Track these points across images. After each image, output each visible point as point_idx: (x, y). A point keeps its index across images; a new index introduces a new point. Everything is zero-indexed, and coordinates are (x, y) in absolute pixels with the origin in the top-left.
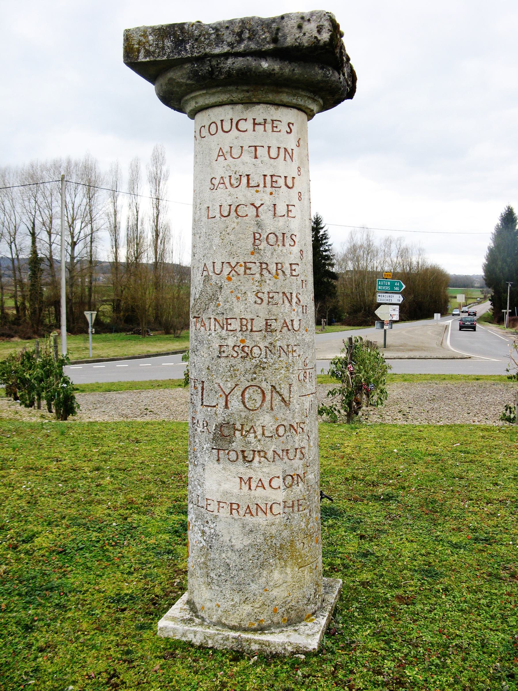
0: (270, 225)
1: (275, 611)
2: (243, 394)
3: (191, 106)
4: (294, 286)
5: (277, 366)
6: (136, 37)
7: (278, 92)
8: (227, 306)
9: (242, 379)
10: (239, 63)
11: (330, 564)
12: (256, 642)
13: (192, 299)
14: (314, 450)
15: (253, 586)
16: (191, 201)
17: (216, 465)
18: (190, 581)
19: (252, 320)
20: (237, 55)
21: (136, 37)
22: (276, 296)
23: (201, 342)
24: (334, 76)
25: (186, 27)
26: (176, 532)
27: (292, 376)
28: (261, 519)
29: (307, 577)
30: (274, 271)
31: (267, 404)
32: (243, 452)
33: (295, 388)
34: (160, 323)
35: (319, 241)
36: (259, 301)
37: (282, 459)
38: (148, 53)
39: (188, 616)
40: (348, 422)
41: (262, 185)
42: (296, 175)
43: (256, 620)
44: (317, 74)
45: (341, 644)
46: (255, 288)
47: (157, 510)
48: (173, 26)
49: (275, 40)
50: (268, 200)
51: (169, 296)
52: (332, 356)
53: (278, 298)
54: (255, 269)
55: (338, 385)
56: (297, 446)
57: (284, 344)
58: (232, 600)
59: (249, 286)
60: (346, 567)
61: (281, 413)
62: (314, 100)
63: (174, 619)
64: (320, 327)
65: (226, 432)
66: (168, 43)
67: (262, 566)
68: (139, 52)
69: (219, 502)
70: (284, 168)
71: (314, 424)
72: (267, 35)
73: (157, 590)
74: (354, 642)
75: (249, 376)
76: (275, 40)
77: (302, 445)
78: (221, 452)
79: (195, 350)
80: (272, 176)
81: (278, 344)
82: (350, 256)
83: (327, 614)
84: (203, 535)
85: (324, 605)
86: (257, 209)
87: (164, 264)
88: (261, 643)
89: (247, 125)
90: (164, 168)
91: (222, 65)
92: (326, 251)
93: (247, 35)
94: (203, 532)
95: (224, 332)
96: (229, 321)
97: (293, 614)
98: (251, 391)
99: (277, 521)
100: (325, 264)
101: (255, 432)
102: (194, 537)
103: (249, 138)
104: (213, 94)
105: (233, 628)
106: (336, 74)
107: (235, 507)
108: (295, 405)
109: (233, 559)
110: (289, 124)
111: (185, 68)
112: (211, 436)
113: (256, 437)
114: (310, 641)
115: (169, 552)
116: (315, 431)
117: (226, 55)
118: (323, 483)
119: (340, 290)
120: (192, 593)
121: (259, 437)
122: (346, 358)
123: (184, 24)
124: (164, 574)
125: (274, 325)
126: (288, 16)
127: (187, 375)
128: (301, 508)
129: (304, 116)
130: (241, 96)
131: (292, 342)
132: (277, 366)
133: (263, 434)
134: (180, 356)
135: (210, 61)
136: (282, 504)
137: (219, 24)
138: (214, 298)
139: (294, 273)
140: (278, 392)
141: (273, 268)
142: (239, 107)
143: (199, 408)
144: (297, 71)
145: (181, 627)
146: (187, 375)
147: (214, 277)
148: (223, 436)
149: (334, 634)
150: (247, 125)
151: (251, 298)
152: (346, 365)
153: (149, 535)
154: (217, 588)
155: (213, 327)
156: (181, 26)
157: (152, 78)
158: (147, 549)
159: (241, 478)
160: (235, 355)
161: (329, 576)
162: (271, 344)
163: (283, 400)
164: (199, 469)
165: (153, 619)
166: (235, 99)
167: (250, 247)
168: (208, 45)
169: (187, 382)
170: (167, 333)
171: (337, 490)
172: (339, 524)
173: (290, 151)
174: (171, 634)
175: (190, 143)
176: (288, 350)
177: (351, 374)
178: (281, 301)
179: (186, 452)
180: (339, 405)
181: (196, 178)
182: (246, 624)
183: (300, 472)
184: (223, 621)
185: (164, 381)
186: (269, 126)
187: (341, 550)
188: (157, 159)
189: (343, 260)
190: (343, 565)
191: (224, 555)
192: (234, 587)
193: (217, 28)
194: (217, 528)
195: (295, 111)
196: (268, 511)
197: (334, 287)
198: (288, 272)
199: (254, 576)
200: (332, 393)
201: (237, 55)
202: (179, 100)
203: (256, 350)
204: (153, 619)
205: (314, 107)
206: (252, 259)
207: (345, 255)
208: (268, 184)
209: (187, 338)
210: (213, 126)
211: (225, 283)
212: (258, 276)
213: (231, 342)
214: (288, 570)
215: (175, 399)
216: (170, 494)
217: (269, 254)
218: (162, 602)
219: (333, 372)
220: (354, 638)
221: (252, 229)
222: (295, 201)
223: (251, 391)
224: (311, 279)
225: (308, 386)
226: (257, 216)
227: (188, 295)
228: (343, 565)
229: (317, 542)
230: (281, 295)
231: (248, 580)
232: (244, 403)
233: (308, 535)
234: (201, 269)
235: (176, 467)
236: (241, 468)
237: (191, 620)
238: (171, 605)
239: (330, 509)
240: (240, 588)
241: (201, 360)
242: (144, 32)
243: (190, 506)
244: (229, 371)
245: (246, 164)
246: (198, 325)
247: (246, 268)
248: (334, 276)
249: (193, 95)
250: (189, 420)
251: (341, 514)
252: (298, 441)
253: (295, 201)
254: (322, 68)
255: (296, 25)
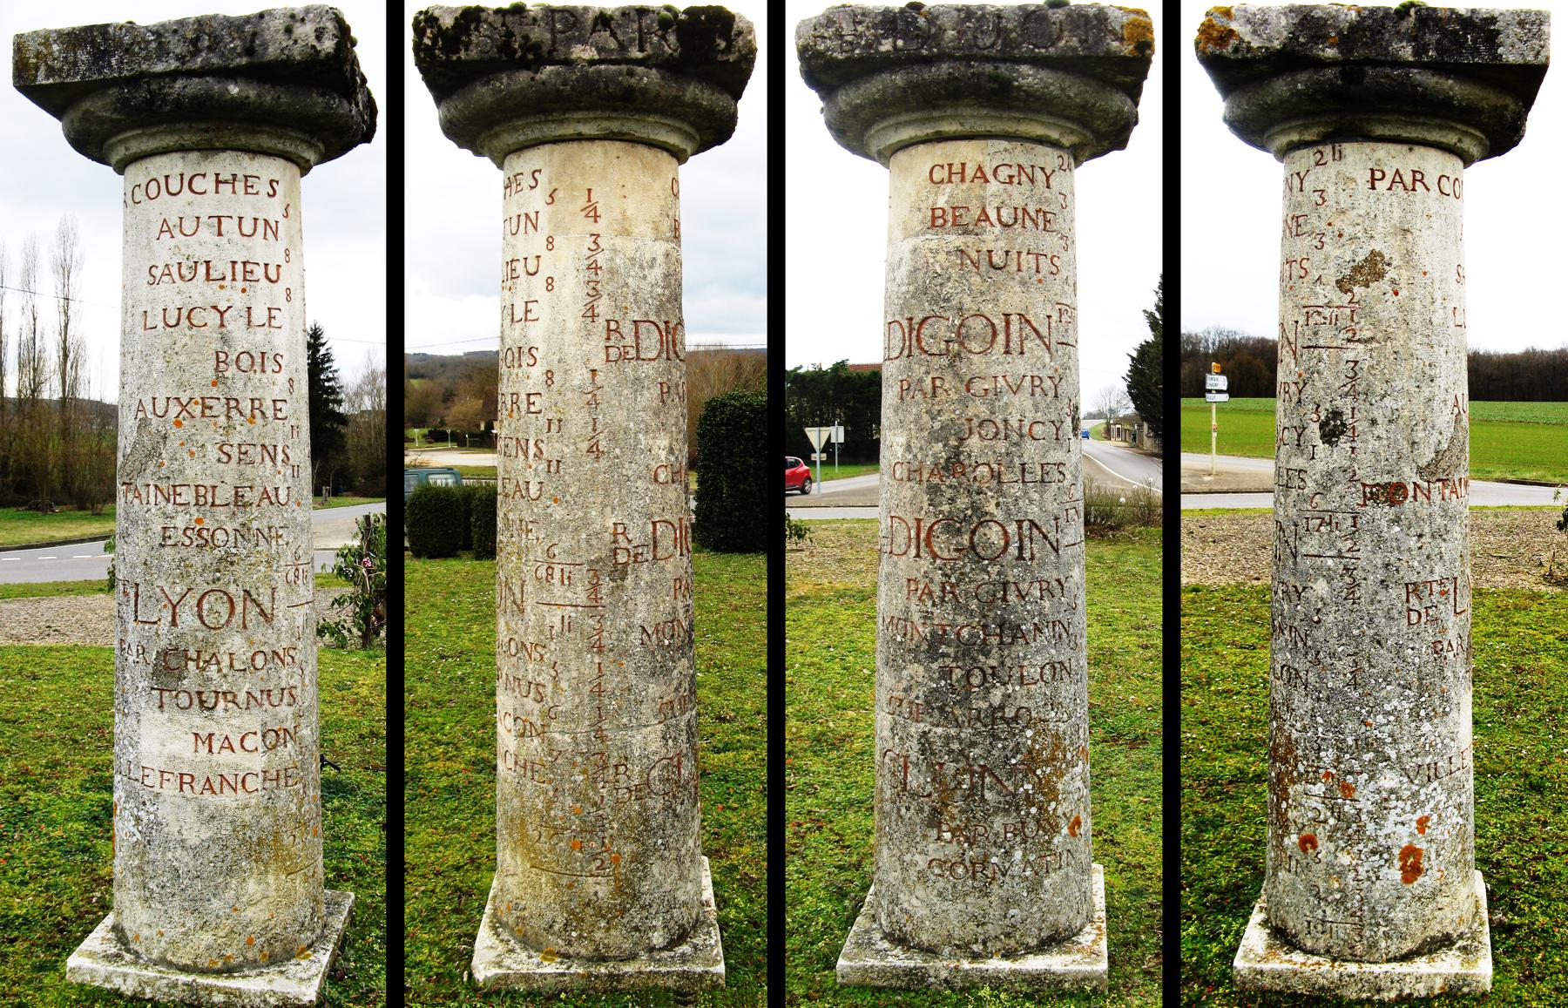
0: (242, 338)
1: (250, 942)
2: (199, 604)
3: (119, 153)
4: (280, 436)
5: (253, 560)
6: (33, 46)
7: (255, 133)
8: (175, 466)
9: (199, 580)
10: (194, 86)
11: (335, 869)
12: (219, 990)
13: (120, 455)
14: (311, 690)
15: (216, 904)
16: (118, 303)
17: (158, 714)
18: (117, 895)
19: (214, 487)
20: (190, 74)
21: (33, 46)
22: (251, 450)
23: (134, 523)
24: (343, 107)
25: (111, 30)
26: (96, 818)
27: (276, 576)
28: (228, 799)
29: (300, 889)
30: (248, 412)
31: (237, 620)
32: (199, 693)
33: (280, 594)
34: (70, 493)
35: (318, 364)
36: (225, 459)
37: (261, 705)
38: (51, 71)
39: (114, 950)
40: (364, 646)
41: (229, 277)
42: (282, 262)
43: (221, 956)
44: (316, 104)
45: (353, 994)
46: (219, 439)
47: (66, 785)
48: (91, 28)
49: (249, 51)
50: (239, 300)
51: (83, 451)
52: (339, 544)
53: (255, 453)
54: (219, 408)
55: (349, 590)
56: (283, 685)
57: (263, 525)
58: (183, 925)
59: (210, 436)
60: (360, 872)
61: (260, 633)
62: (311, 146)
63: (91, 955)
64: (320, 499)
65: (173, 663)
66: (83, 56)
67: (230, 872)
68: (37, 69)
69: (162, 772)
70: (263, 251)
71: (310, 651)
72: (238, 42)
73: (66, 910)
74: (372, 991)
75: (209, 576)
76: (249, 51)
77: (292, 682)
78: (166, 694)
79: (125, 535)
80: (244, 263)
81: (255, 525)
82: (367, 388)
83: (331, 947)
84: (137, 824)
85: (326, 932)
86: (222, 314)
87: (77, 400)
88: (228, 992)
89: (207, 184)
90: (77, 252)
91: (167, 90)
92: (329, 380)
93: (206, 43)
94: (138, 819)
95: (170, 506)
96: (178, 490)
97: (278, 947)
98: (212, 599)
99: (254, 801)
100: (327, 401)
101: (218, 663)
102: (123, 826)
103: (208, 205)
104: (153, 135)
105: (184, 969)
106: (346, 104)
107: (187, 779)
108: (281, 621)
109: (184, 860)
110: (271, 182)
111: (110, 97)
112: (150, 669)
113: (220, 670)
114: (303, 989)
115: (85, 850)
116: (312, 661)
117: (174, 75)
118: (324, 742)
119: (350, 442)
120: (120, 914)
121: (225, 671)
122: (361, 547)
123: (108, 25)
124: (76, 884)
125: (248, 496)
126: (270, 13)
127: (112, 573)
128: (290, 782)
129: (296, 170)
130: (196, 138)
131: (276, 522)
132: (253, 560)
133: (231, 666)
134: (102, 544)
135: (149, 84)
136: (261, 775)
137: (163, 25)
138: (153, 453)
139: (279, 415)
140: (254, 601)
141: (246, 406)
142: (194, 156)
143: (131, 625)
144: (283, 99)
145: (103, 968)
146: (112, 573)
147: (155, 420)
148: (168, 669)
149: (342, 979)
150: (207, 184)
151: (213, 453)
152: (361, 557)
153: (53, 823)
154: (159, 906)
155: (152, 499)
156: (103, 29)
157: (57, 111)
158: (50, 845)
159: (196, 735)
160: (188, 542)
161: (333, 887)
162: (244, 525)
163: (262, 612)
164: (131, 720)
165: (59, 955)
166: (187, 143)
167: (211, 374)
168: (146, 58)
169: (112, 585)
170: (82, 508)
171: (346, 753)
172: (350, 806)
173: (273, 225)
174: (88, 978)
175: (115, 214)
176: (270, 535)
177: (369, 572)
178: (259, 459)
179: (111, 694)
180: (349, 620)
181: (126, 265)
182: (204, 962)
183: (289, 725)
184: (169, 957)
185: (76, 583)
186: (240, 186)
187: (352, 847)
188: (66, 238)
189: (356, 394)
190: (356, 870)
191: (170, 855)
192: (186, 904)
193: (158, 32)
194: (159, 813)
195: (280, 163)
196: (239, 786)
197: (342, 436)
198: (270, 413)
199: (216, 887)
200: (339, 602)
201: (190, 74)
202: (101, 144)
203: (220, 535)
204: (59, 955)
205: (311, 156)
206: (214, 392)
207: (360, 387)
208: (240, 276)
209: (112, 516)
210: (153, 185)
211: (172, 430)
212: (223, 419)
213: (180, 522)
214: (271, 878)
215: (94, 611)
216: (85, 760)
217: (240, 385)
218: (74, 927)
219: (341, 569)
220: (373, 985)
221: (213, 346)
222: (281, 301)
223: (212, 599)
224: (305, 424)
225: (302, 590)
226: (222, 325)
227: (115, 448)
228: (356, 870)
229: (316, 834)
230: (259, 448)
231: (207, 894)
232: (201, 617)
233: (301, 824)
234: (134, 408)
235: (95, 717)
236: (197, 720)
237: (118, 956)
238: (87, 933)
239: (336, 782)
240: (195, 905)
241: (134, 550)
242: (46, 39)
243: (118, 778)
244: (178, 567)
245: (204, 245)
246: (130, 496)
247: (205, 407)
248: (342, 419)
249: (121, 136)
250: (116, 644)
251: (353, 791)
252: (285, 676)
253: (281, 301)
254: (323, 95)
255: (282, 28)
